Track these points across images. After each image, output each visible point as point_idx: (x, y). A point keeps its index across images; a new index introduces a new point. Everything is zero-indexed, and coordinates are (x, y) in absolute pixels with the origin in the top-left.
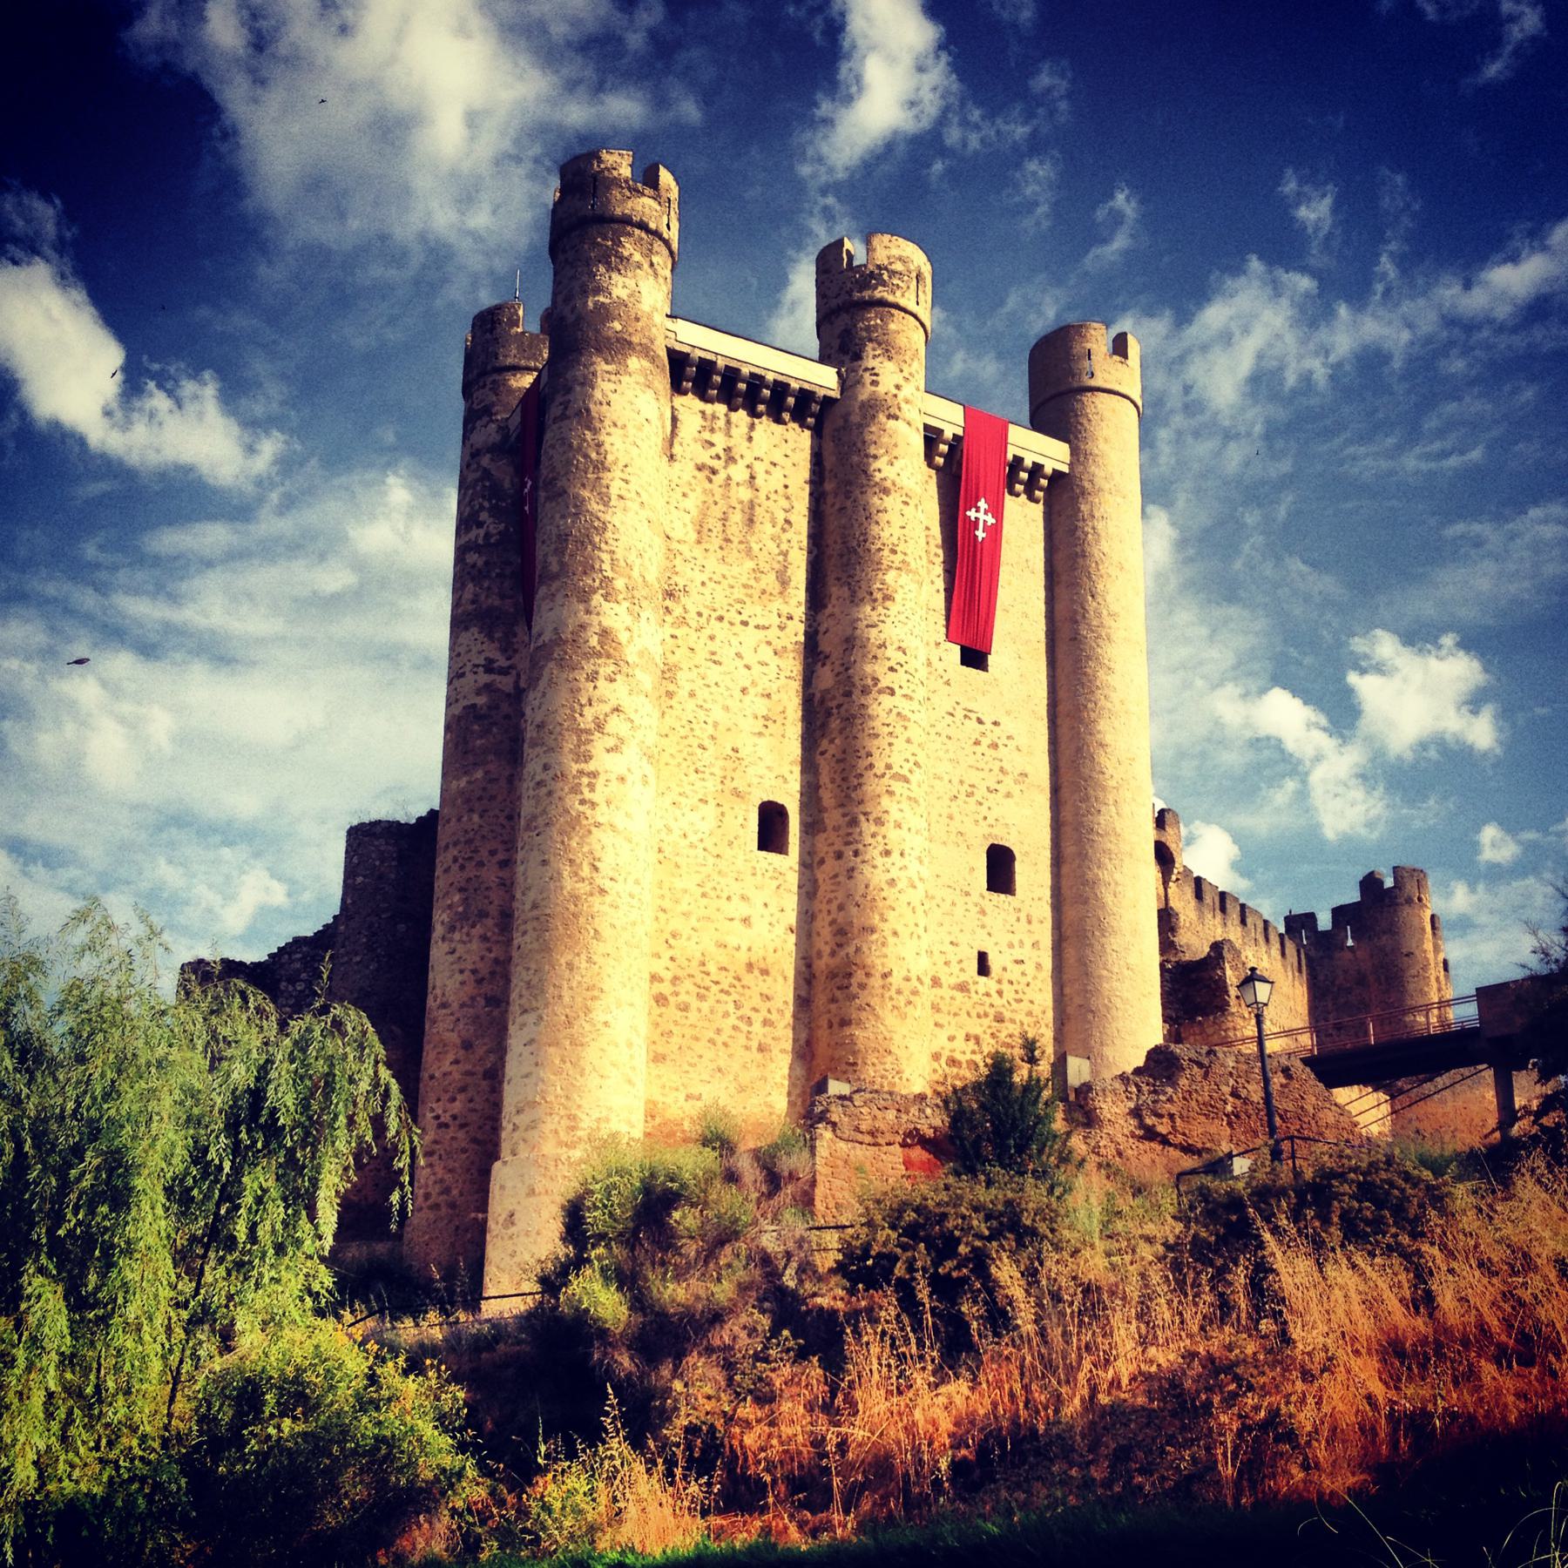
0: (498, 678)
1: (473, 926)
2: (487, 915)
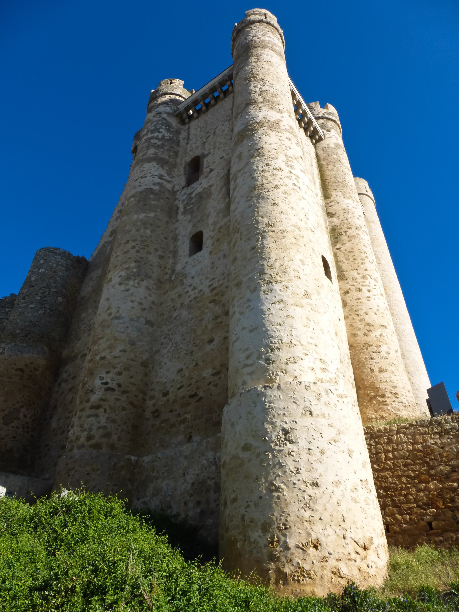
0: (165, 183)
1: (142, 280)
2: (150, 277)
